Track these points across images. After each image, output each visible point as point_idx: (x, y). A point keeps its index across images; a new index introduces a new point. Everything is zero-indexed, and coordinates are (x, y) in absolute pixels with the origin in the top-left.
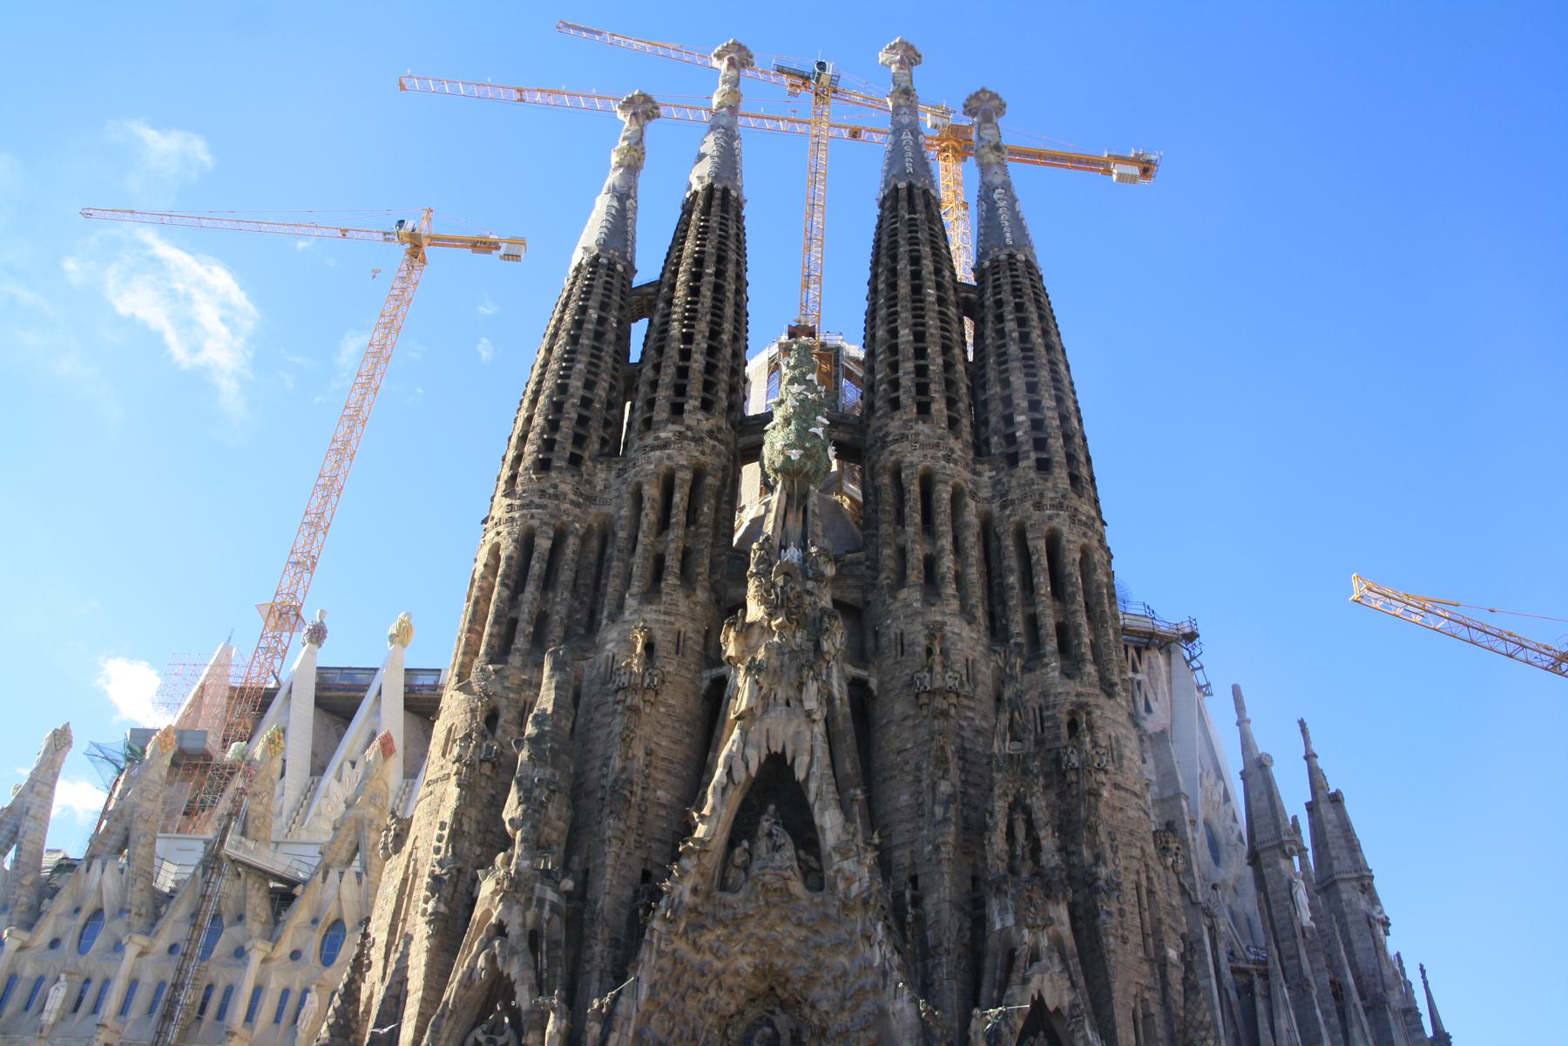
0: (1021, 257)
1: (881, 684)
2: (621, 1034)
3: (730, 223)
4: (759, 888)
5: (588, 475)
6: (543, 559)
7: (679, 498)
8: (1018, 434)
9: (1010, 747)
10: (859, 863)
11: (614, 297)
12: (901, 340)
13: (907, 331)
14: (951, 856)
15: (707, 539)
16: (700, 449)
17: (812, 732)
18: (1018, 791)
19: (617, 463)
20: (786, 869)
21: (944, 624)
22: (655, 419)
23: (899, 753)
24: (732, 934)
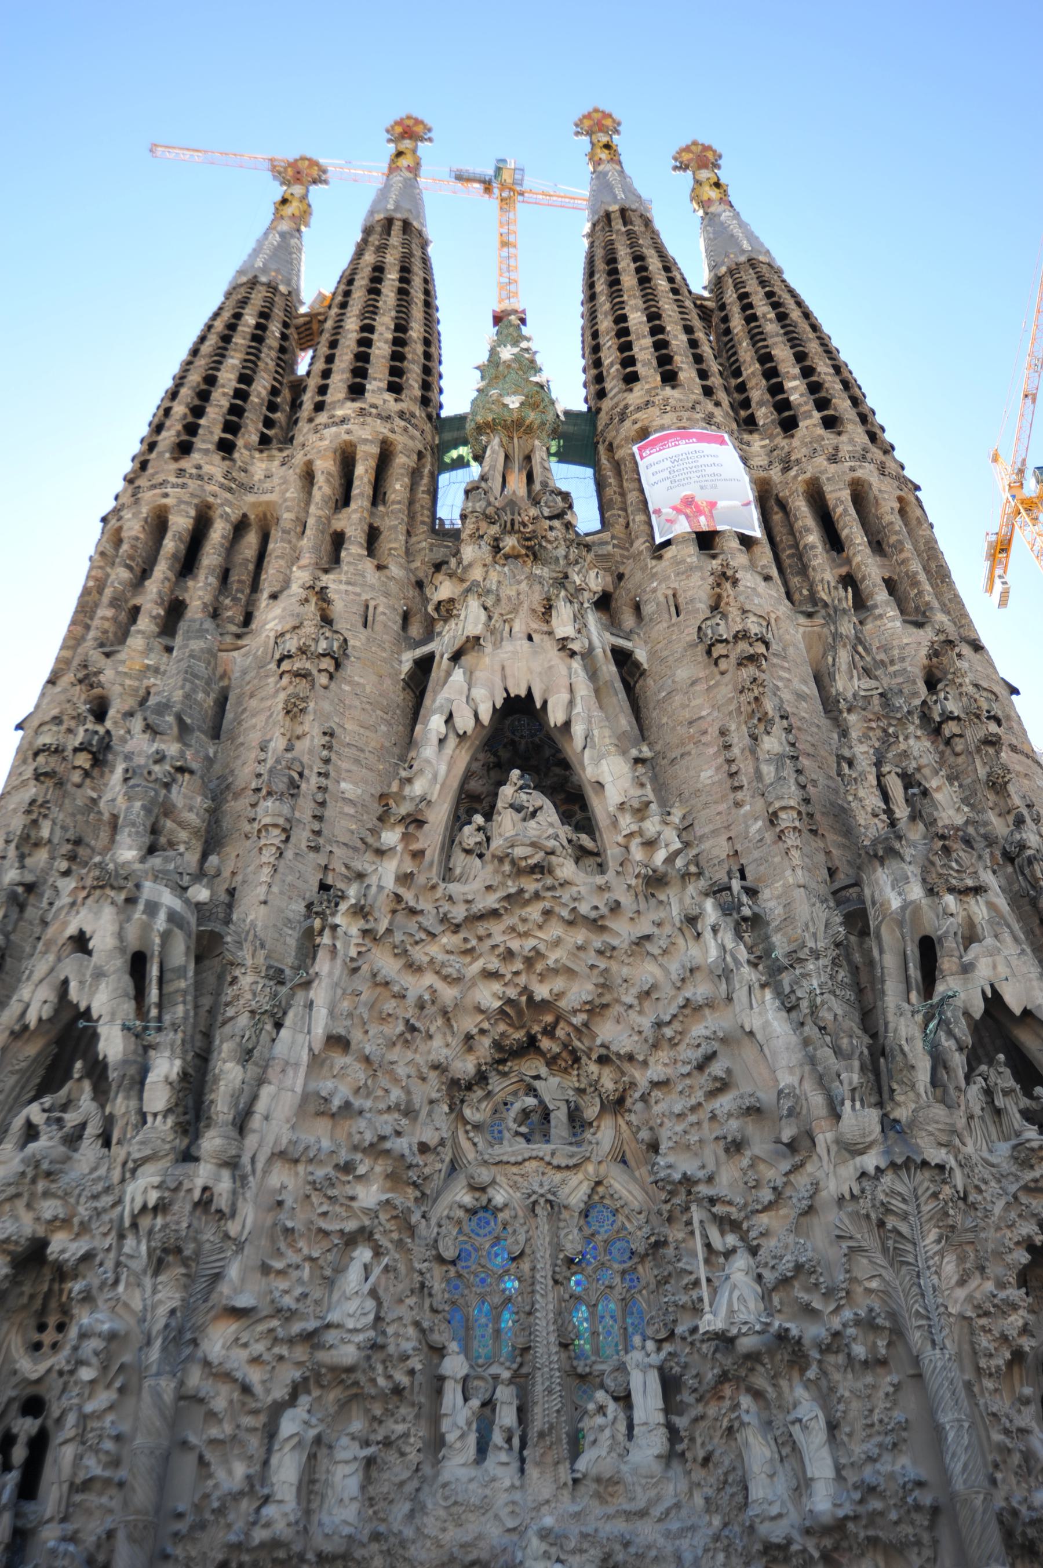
1: (652, 654)
2: (280, 1089)
3: (414, 246)
4: (507, 867)
6: (180, 539)
7: (363, 471)
8: (792, 398)
11: (276, 311)
17: (570, 668)
18: (885, 731)
19: (281, 450)
23: (690, 723)
24: (466, 940)
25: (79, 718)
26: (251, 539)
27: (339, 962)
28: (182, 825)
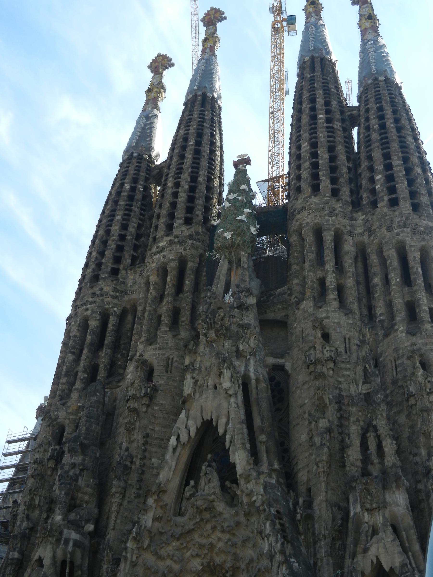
0: (382, 78)
4: (195, 510)
5: (122, 278)
6: (93, 333)
8: (377, 187)
9: (363, 389)
10: (257, 483)
11: (141, 174)
12: (303, 150)
13: (306, 143)
14: (325, 468)
15: (188, 300)
16: (183, 247)
17: (229, 402)
19: (139, 267)
20: (211, 495)
21: (328, 318)
22: (157, 237)
23: (301, 407)
25: (50, 444)
26: (130, 318)
27: (128, 563)
28: (85, 493)
